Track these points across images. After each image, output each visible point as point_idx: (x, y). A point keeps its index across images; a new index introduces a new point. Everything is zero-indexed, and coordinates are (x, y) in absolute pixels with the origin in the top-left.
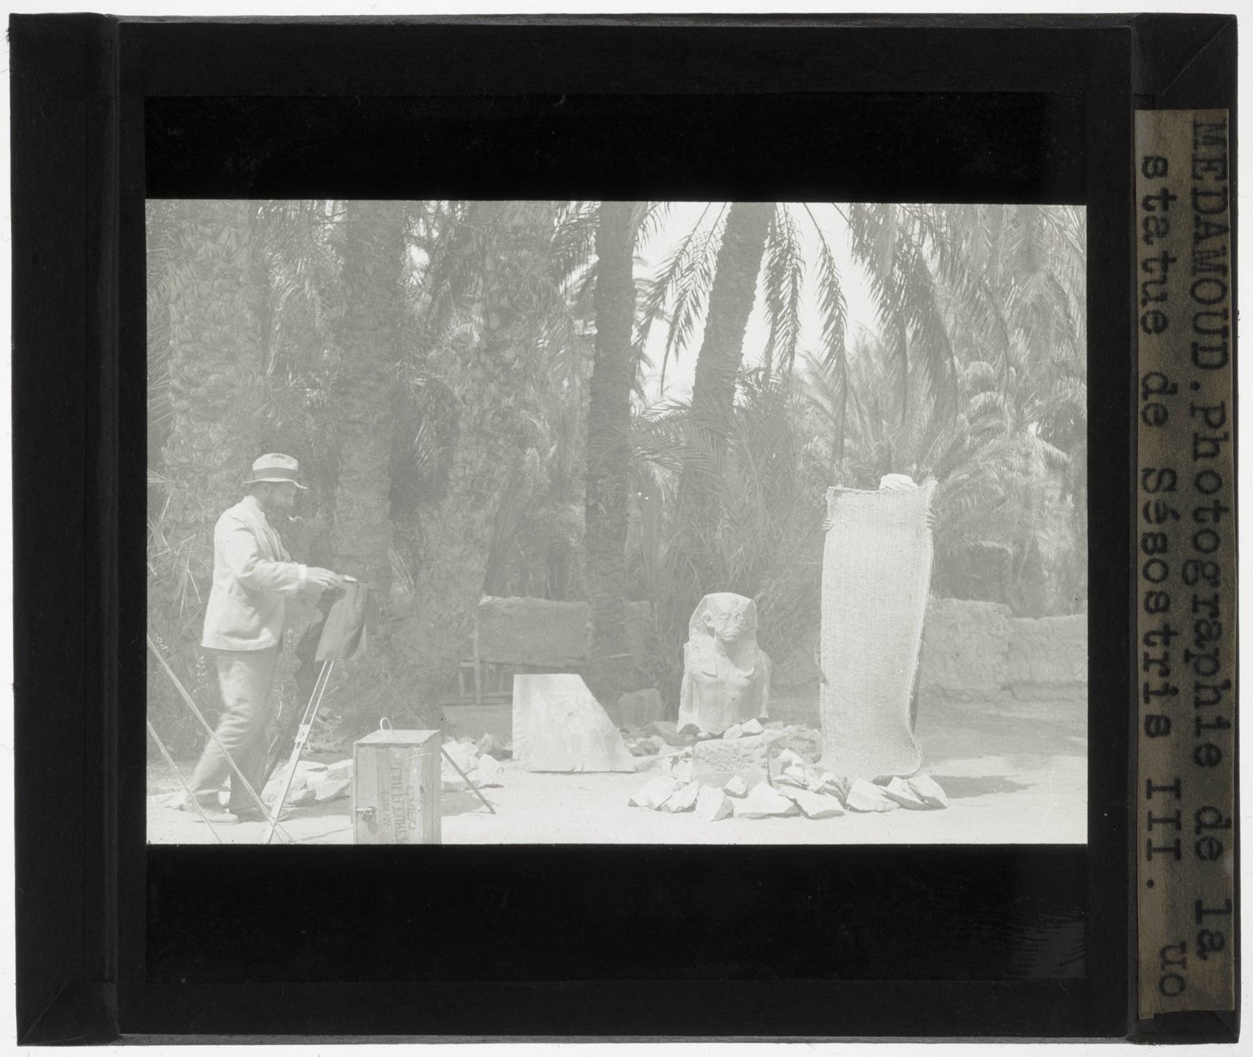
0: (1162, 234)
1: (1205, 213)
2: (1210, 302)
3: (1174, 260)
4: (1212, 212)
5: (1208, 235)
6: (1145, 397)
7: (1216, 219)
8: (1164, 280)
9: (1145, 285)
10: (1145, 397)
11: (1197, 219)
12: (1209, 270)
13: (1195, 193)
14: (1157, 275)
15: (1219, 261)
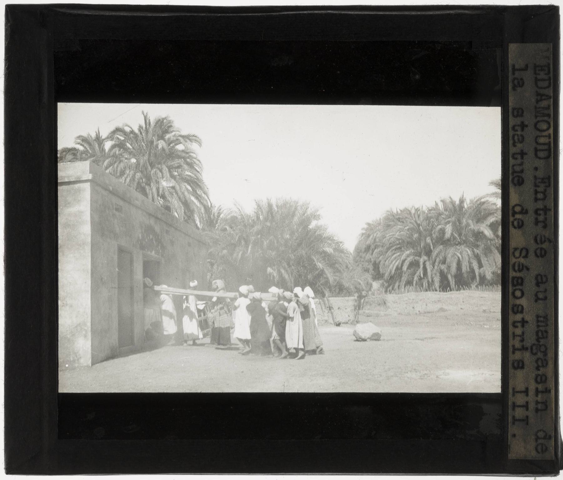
0: (521, 142)
1: (541, 88)
2: (544, 131)
3: (527, 126)
4: (545, 88)
5: (541, 100)
6: (513, 216)
7: (546, 92)
8: (521, 164)
9: (513, 166)
10: (513, 216)
11: (537, 92)
12: (544, 116)
13: (536, 80)
14: (519, 161)
15: (546, 112)
